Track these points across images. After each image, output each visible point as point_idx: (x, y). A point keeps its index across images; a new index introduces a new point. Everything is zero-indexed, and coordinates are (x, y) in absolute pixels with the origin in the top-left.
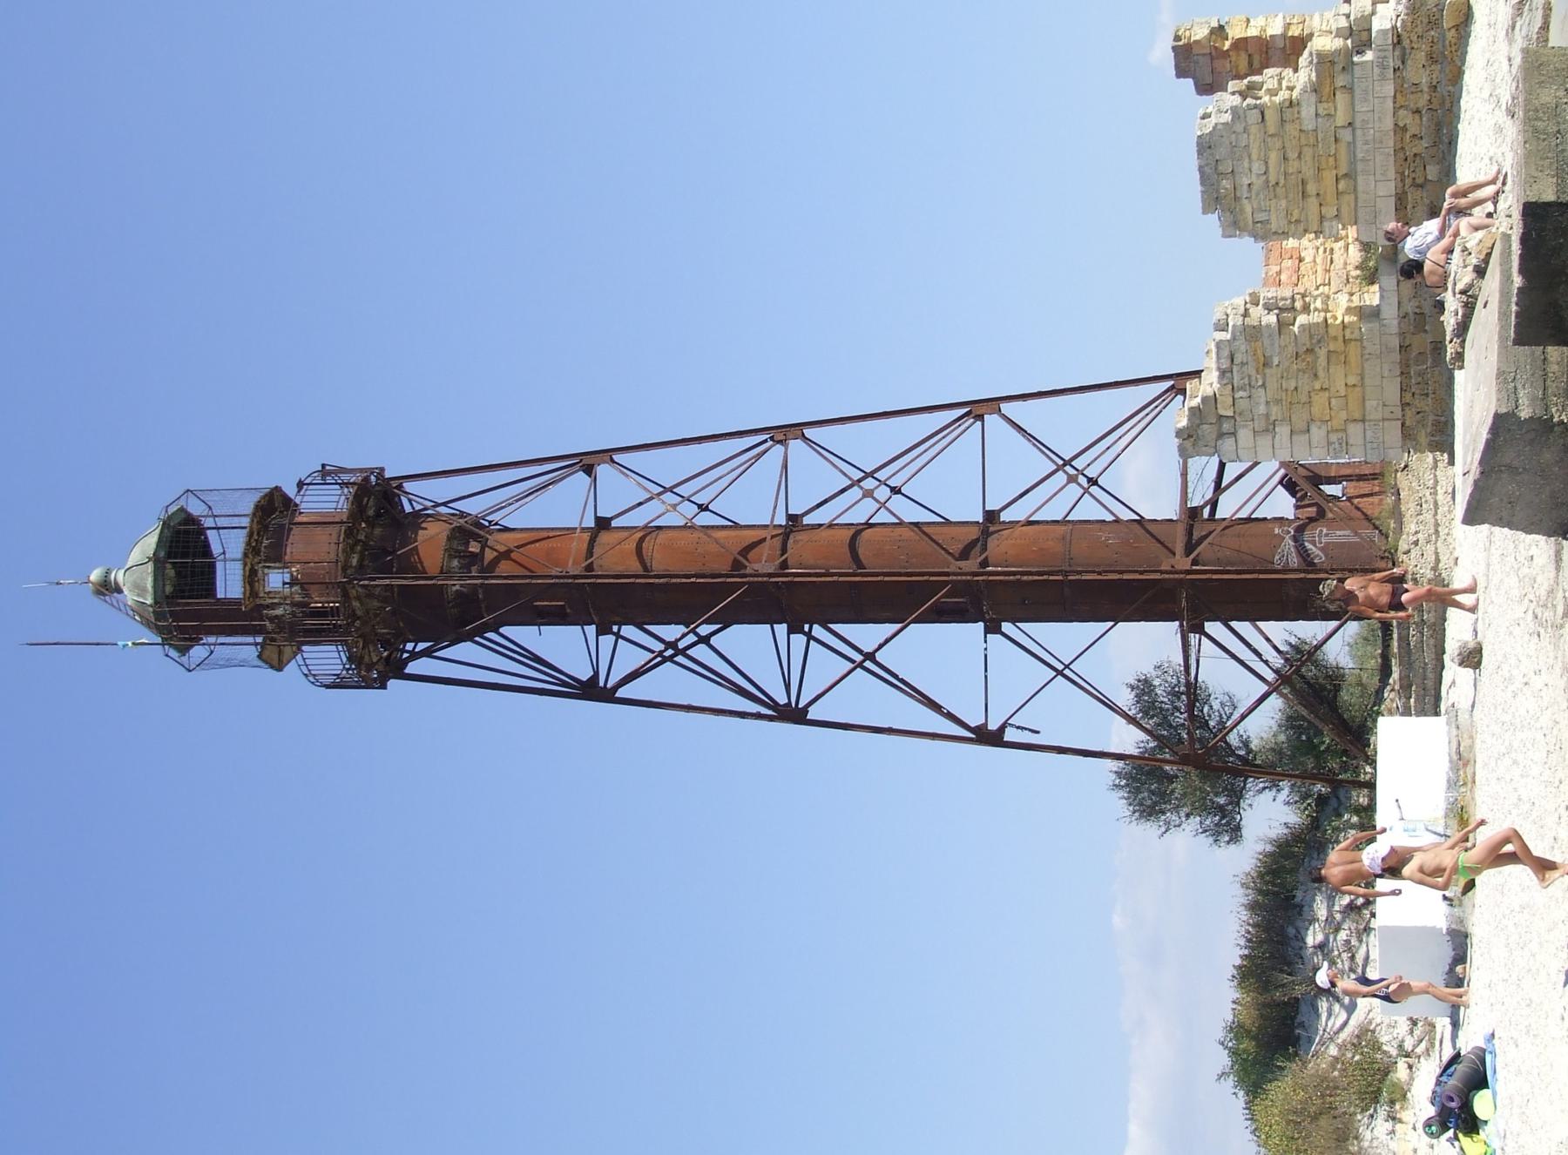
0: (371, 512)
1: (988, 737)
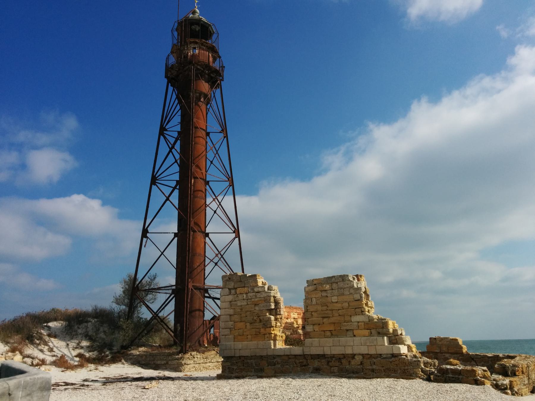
0: (212, 75)
1: (145, 233)
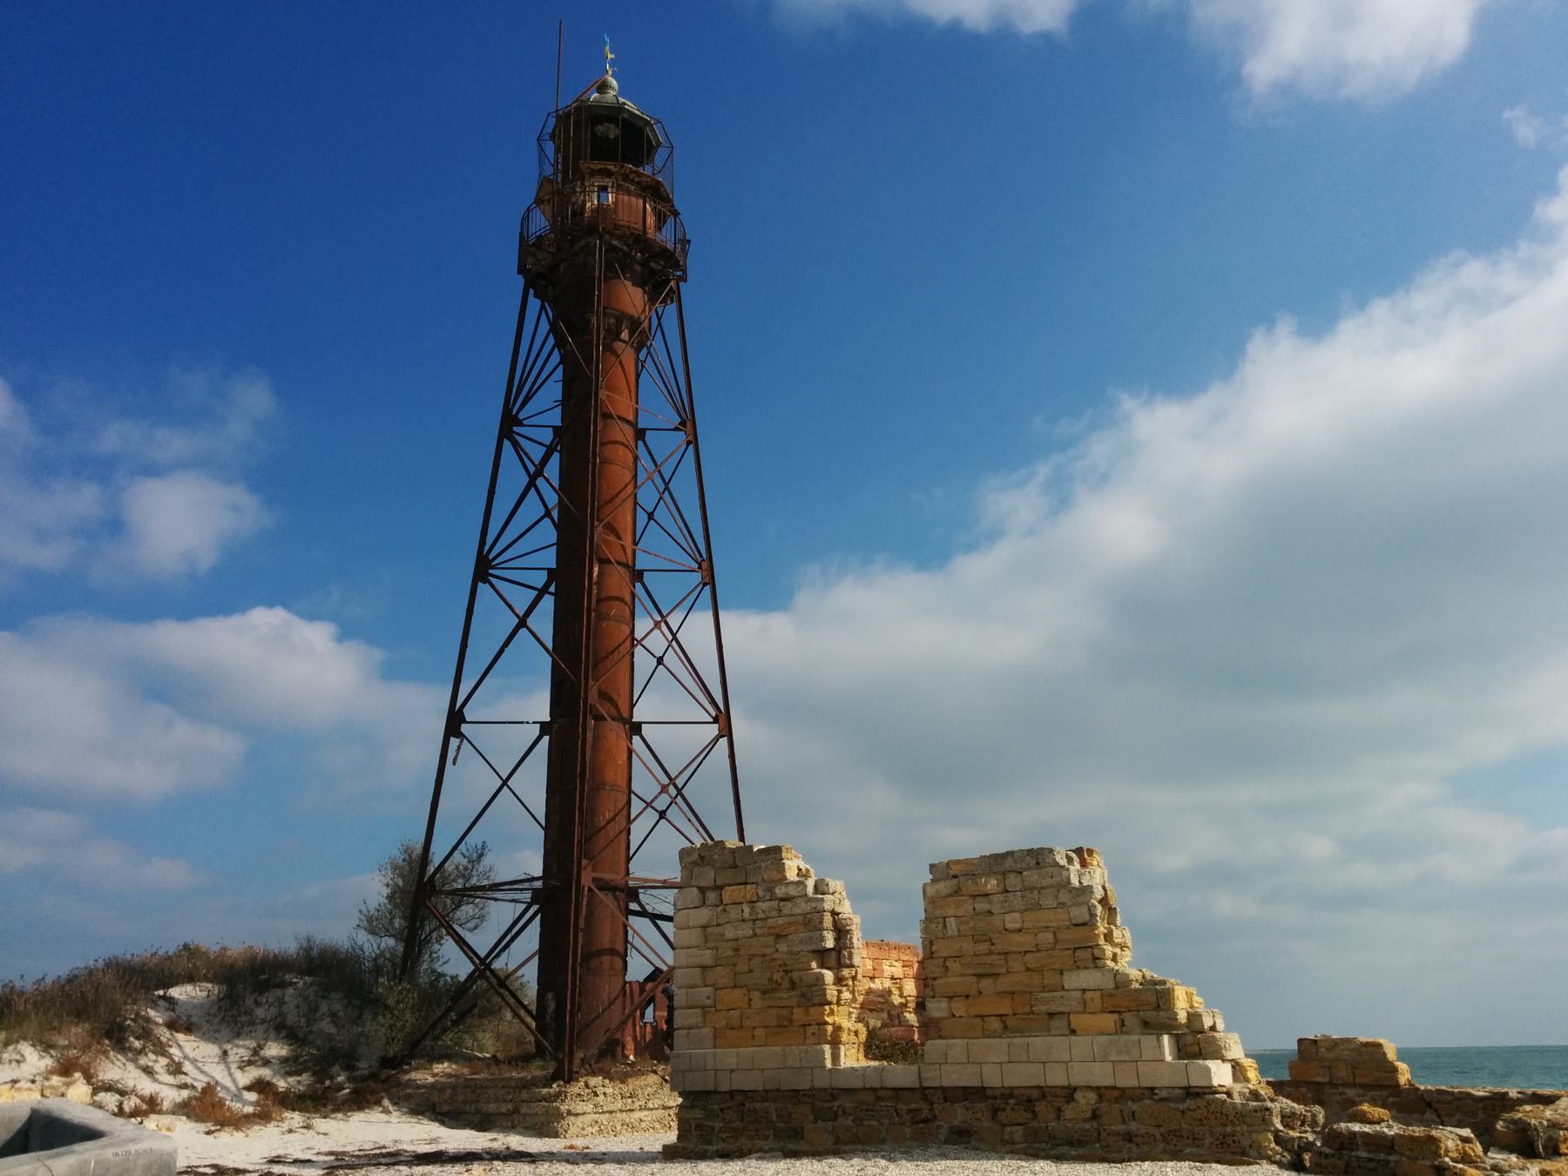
1: (455, 722)
